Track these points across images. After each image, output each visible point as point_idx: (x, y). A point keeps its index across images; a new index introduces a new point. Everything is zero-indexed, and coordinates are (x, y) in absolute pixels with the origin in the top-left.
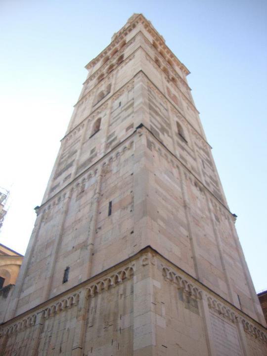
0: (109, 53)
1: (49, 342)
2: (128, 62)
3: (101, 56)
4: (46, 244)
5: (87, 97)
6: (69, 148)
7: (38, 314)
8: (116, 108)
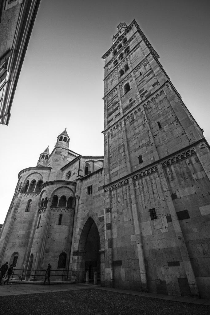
0: (116, 47)
1: (143, 190)
2: (136, 50)
3: (111, 50)
4: (117, 147)
5: (112, 73)
6: (111, 101)
7: (129, 179)
8: (138, 76)
